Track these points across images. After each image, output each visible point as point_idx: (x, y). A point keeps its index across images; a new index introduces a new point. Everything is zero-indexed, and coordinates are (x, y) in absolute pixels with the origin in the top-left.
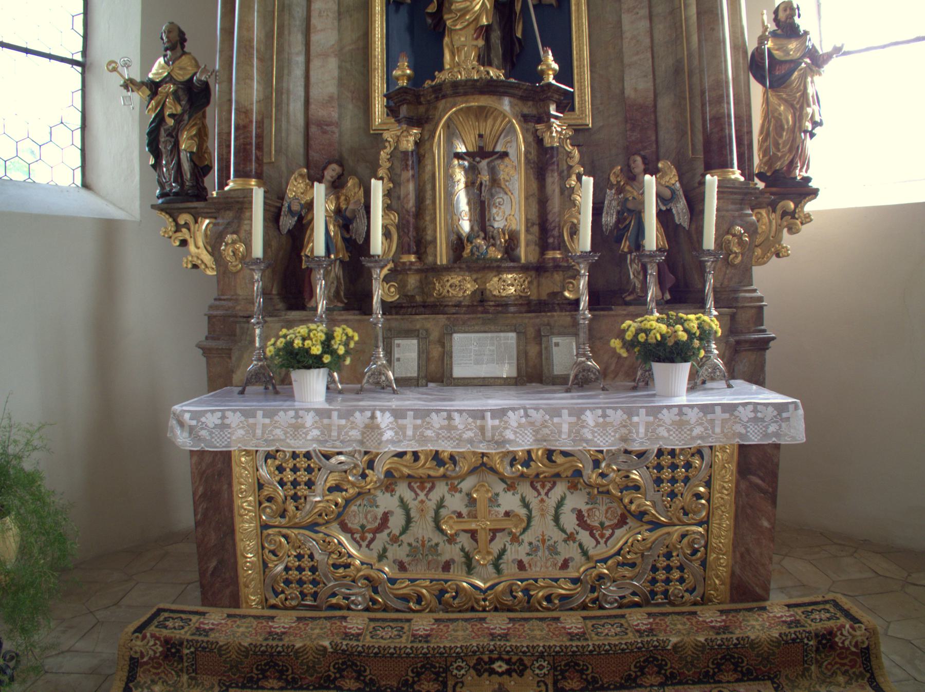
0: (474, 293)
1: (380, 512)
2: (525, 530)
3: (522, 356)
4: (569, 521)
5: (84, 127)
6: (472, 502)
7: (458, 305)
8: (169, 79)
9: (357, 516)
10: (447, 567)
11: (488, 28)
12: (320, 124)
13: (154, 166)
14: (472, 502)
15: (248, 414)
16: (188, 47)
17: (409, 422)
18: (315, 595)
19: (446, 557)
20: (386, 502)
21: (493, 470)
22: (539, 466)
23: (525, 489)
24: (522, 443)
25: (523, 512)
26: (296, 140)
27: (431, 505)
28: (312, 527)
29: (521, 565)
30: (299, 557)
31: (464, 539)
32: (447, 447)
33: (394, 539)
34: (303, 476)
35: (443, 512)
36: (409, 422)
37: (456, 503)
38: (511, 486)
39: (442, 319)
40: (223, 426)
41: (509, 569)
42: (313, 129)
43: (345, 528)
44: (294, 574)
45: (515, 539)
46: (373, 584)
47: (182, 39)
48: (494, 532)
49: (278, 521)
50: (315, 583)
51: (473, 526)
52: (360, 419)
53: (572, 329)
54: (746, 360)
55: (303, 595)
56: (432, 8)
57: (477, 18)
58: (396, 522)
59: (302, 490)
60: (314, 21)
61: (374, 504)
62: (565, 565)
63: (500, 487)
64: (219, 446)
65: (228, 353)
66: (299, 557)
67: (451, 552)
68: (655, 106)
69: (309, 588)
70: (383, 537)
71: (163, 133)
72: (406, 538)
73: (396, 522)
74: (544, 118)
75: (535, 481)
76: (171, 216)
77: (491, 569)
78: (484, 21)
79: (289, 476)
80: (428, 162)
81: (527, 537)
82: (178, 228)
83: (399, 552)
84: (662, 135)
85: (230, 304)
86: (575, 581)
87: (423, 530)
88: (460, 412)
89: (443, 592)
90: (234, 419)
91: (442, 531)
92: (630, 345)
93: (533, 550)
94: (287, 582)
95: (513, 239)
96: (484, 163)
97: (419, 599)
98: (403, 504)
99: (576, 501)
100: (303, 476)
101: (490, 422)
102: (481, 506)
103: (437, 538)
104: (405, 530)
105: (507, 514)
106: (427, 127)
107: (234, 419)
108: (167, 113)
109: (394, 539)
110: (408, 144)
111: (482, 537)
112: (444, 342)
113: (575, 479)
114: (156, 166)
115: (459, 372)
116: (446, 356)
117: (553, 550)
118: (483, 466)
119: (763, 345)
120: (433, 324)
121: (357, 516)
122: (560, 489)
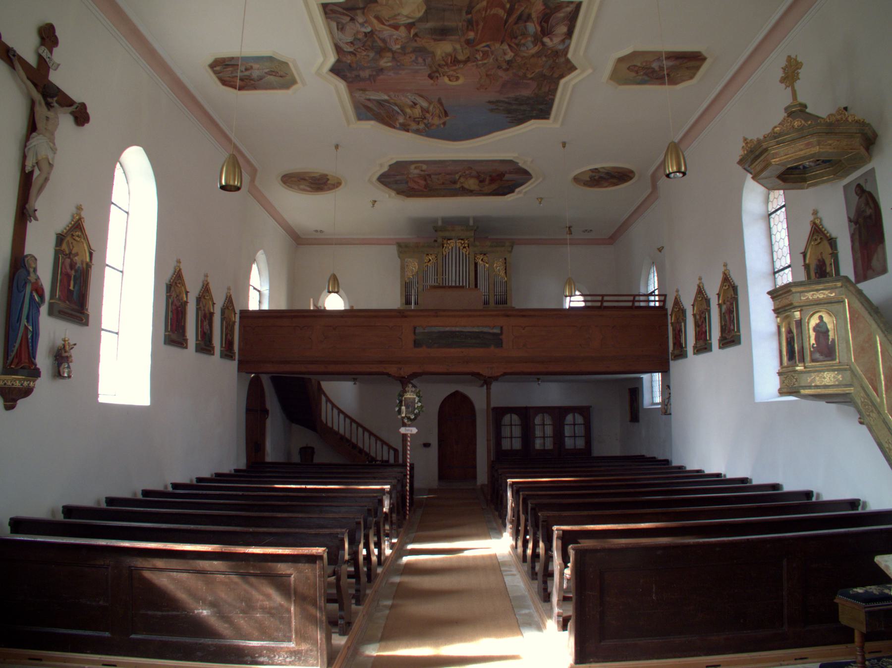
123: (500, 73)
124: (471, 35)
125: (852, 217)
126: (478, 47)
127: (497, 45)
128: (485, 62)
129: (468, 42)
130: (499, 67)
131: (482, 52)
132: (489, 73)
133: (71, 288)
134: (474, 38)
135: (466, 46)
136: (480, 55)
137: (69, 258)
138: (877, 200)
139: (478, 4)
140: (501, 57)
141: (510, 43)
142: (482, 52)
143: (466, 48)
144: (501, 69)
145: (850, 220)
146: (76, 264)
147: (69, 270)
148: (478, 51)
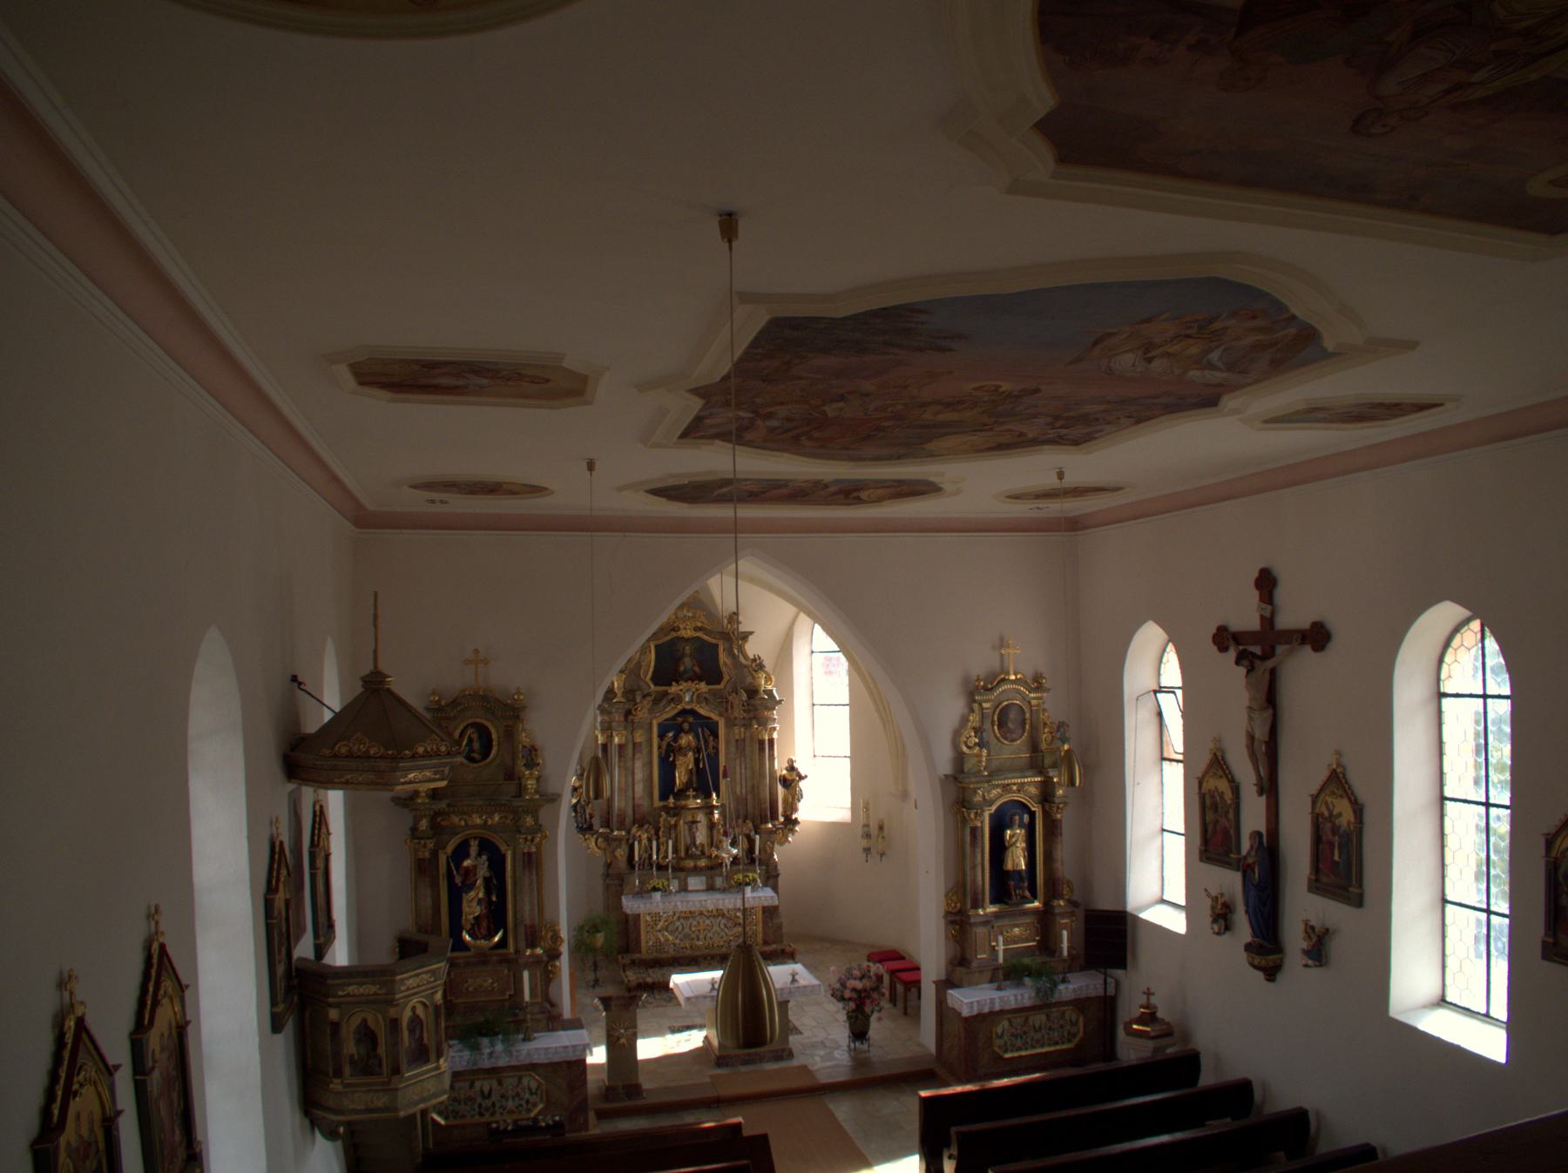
3: (707, 884)
4: (722, 926)
6: (698, 923)
7: (689, 869)
10: (693, 939)
11: (691, 769)
12: (639, 806)
14: (698, 923)
15: (645, 904)
17: (685, 903)
20: (678, 924)
22: (715, 912)
23: (711, 919)
24: (711, 907)
26: (630, 812)
28: (660, 931)
31: (697, 933)
32: (693, 909)
36: (685, 903)
37: (695, 923)
38: (708, 918)
40: (639, 907)
41: (708, 939)
42: (636, 808)
43: (667, 930)
46: (674, 944)
48: (704, 930)
52: (673, 904)
53: (721, 875)
54: (771, 881)
56: (671, 759)
57: (688, 766)
58: (680, 929)
60: (636, 771)
62: (722, 937)
63: (705, 918)
64: (637, 912)
65: (621, 885)
67: (694, 936)
68: (746, 799)
70: (677, 933)
71: (578, 806)
73: (680, 929)
74: (712, 813)
75: (714, 916)
78: (690, 767)
80: (679, 828)
81: (713, 930)
83: (681, 936)
84: (749, 807)
86: (724, 941)
87: (687, 930)
90: (641, 905)
92: (736, 882)
93: (714, 934)
95: (703, 845)
96: (694, 826)
97: (686, 948)
98: (682, 924)
99: (724, 921)
101: (703, 903)
102: (702, 923)
103: (690, 932)
107: (641, 905)
108: (582, 800)
109: (680, 933)
110: (673, 822)
112: (685, 880)
113: (723, 915)
114: (576, 817)
115: (690, 888)
116: (686, 885)
117: (719, 934)
118: (701, 913)
119: (778, 875)
120: (682, 875)
121: (670, 928)
122: (720, 918)
133: (1336, 857)
137: (1331, 822)
146: (1340, 827)
147: (1330, 837)
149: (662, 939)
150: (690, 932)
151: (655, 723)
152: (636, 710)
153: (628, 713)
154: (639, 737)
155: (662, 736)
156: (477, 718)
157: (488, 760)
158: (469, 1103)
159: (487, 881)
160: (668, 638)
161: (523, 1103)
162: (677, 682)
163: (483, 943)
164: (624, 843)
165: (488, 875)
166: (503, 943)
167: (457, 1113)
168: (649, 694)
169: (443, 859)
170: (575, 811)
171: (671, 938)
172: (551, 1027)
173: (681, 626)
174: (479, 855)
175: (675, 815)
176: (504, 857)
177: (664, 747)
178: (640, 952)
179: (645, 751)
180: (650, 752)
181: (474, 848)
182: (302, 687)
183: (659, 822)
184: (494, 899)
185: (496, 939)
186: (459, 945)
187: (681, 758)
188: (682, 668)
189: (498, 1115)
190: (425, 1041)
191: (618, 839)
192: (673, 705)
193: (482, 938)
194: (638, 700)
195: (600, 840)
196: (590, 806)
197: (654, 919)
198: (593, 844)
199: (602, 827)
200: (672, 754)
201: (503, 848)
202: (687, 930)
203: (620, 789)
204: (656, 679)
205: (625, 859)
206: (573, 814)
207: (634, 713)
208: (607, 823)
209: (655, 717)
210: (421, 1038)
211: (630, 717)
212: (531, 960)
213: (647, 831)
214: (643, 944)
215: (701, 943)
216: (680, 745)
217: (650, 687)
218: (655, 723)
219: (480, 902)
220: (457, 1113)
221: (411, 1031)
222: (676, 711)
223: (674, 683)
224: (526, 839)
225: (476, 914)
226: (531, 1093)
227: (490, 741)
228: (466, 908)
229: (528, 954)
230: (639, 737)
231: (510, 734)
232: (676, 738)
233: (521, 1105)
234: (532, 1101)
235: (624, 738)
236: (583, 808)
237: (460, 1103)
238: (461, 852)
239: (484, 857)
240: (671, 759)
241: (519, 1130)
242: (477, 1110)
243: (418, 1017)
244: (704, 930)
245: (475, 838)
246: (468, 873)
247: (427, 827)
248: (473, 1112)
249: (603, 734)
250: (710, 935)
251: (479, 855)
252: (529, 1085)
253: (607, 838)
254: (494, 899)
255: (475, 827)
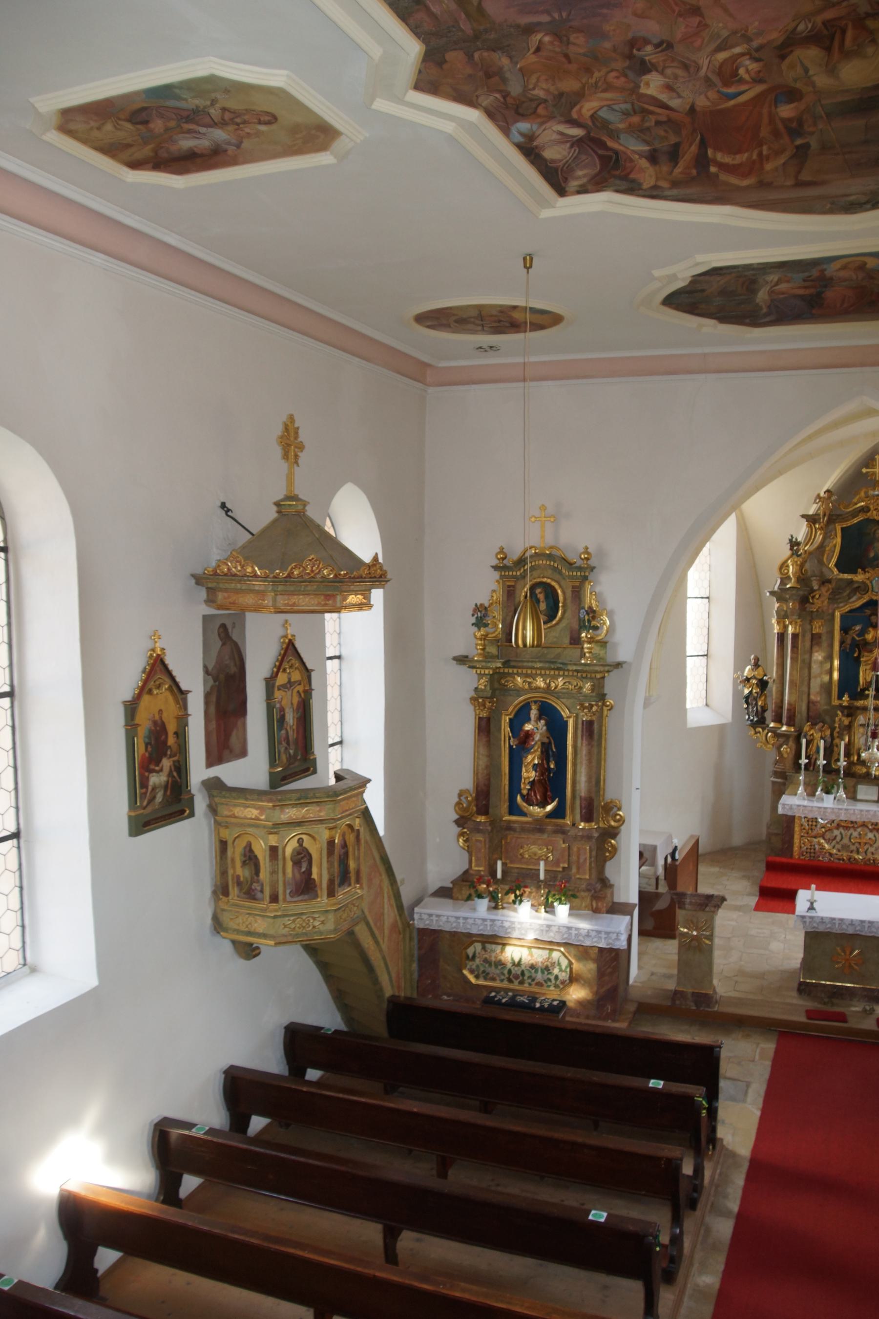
0: (865, 773)
1: (834, 835)
2: (875, 843)
5: (707, 681)
6: (860, 834)
8: (754, 677)
9: (828, 835)
12: (814, 703)
13: (746, 708)
16: (760, 663)
18: (814, 857)
19: (851, 849)
20: (836, 832)
21: (867, 826)
25: (874, 838)
27: (849, 834)
29: (873, 854)
30: (811, 846)
31: (857, 845)
32: (853, 819)
33: (838, 843)
34: (814, 823)
35: (852, 836)
37: (855, 834)
38: (871, 831)
39: (854, 780)
42: (811, 705)
43: (824, 839)
44: (808, 850)
45: (871, 846)
46: (831, 854)
47: (758, 660)
48: (866, 843)
49: (806, 835)
50: (814, 853)
51: (859, 841)
55: (810, 856)
56: (856, 655)
58: (838, 838)
59: (813, 827)
61: (832, 832)
64: (790, 814)
65: (784, 784)
66: (811, 846)
67: (853, 848)
69: (812, 855)
70: (834, 842)
72: (842, 843)
73: (838, 838)
76: (754, 728)
77: (864, 854)
79: (810, 823)
81: (875, 845)
82: (756, 733)
83: (839, 846)
85: (783, 767)
88: (857, 810)
89: (850, 858)
91: (851, 842)
94: (807, 853)
98: (841, 834)
100: (814, 823)
103: (849, 844)
104: (841, 840)
105: (870, 839)
106: (854, 718)
108: (754, 691)
109: (838, 843)
111: (862, 844)
114: (747, 708)
115: (859, 797)
116: (855, 792)
118: (864, 825)
120: (851, 782)
121: (828, 835)
123: (652, 28)
124: (786, 111)
125: (210, 668)
126: (759, 89)
127: (702, 102)
128: (722, 56)
129: (792, 95)
130: (664, 46)
131: (741, 81)
132: (696, 20)
134: (776, 107)
135: (798, 85)
136: (747, 71)
138: (244, 658)
139: (784, 164)
140: (676, 77)
141: (667, 112)
142: (741, 81)
143: (795, 80)
144: (655, 41)
145: (207, 671)
148: (758, 80)
149: (817, 847)
150: (849, 844)
151: (837, 614)
152: (813, 597)
153: (804, 601)
154: (818, 627)
155: (845, 630)
156: (543, 577)
157: (554, 622)
158: (500, 967)
159: (545, 749)
160: (855, 521)
161: (552, 978)
162: (864, 570)
163: (536, 810)
164: (791, 739)
165: (546, 740)
166: (558, 813)
167: (488, 974)
168: (829, 581)
169: (505, 720)
170: (747, 702)
171: (827, 846)
172: (594, 905)
173: (871, 507)
174: (539, 718)
175: (848, 716)
176: (566, 724)
177: (849, 641)
178: (791, 856)
179: (825, 644)
180: (831, 646)
181: (534, 713)
182: (230, 513)
183: (834, 722)
184: (552, 766)
185: (549, 808)
186: (514, 809)
187: (866, 654)
188: (872, 555)
189: (526, 985)
190: (315, 876)
191: (785, 736)
192: (858, 595)
193: (537, 805)
194: (816, 587)
195: (770, 734)
196: (763, 698)
197: (810, 823)
198: (764, 738)
199: (773, 721)
200: (857, 649)
201: (565, 713)
202: (846, 841)
203: (791, 681)
204: (842, 566)
205: (791, 756)
206: (745, 706)
207: (811, 601)
208: (778, 719)
209: (838, 608)
210: (309, 872)
211: (807, 605)
212: (580, 834)
213: (821, 731)
214: (796, 848)
215: (861, 857)
216: (865, 640)
217: (833, 573)
218: (837, 614)
219: (535, 767)
220: (488, 974)
221: (297, 863)
222: (858, 604)
223: (859, 570)
224: (583, 707)
225: (531, 780)
226: (561, 970)
227: (556, 601)
228: (524, 774)
229: (580, 827)
230: (818, 627)
231: (577, 594)
232: (862, 633)
233: (550, 980)
234: (560, 978)
235: (798, 627)
236: (755, 699)
237: (490, 965)
238: (522, 714)
239: (543, 722)
240: (856, 655)
241: (513, 1004)
242: (507, 975)
243: (306, 850)
244: (866, 843)
245: (535, 702)
246: (528, 735)
247: (485, 686)
248: (503, 977)
249: (778, 623)
250: (871, 849)
251: (539, 718)
252: (559, 961)
253: (777, 735)
254: (552, 766)
255: (538, 688)
